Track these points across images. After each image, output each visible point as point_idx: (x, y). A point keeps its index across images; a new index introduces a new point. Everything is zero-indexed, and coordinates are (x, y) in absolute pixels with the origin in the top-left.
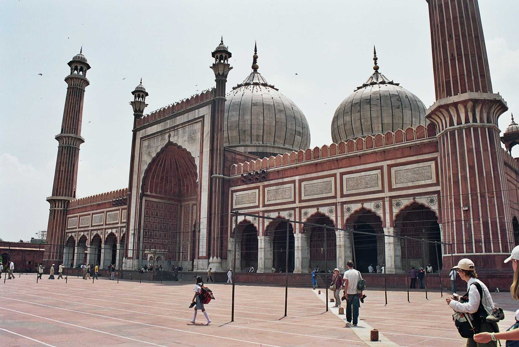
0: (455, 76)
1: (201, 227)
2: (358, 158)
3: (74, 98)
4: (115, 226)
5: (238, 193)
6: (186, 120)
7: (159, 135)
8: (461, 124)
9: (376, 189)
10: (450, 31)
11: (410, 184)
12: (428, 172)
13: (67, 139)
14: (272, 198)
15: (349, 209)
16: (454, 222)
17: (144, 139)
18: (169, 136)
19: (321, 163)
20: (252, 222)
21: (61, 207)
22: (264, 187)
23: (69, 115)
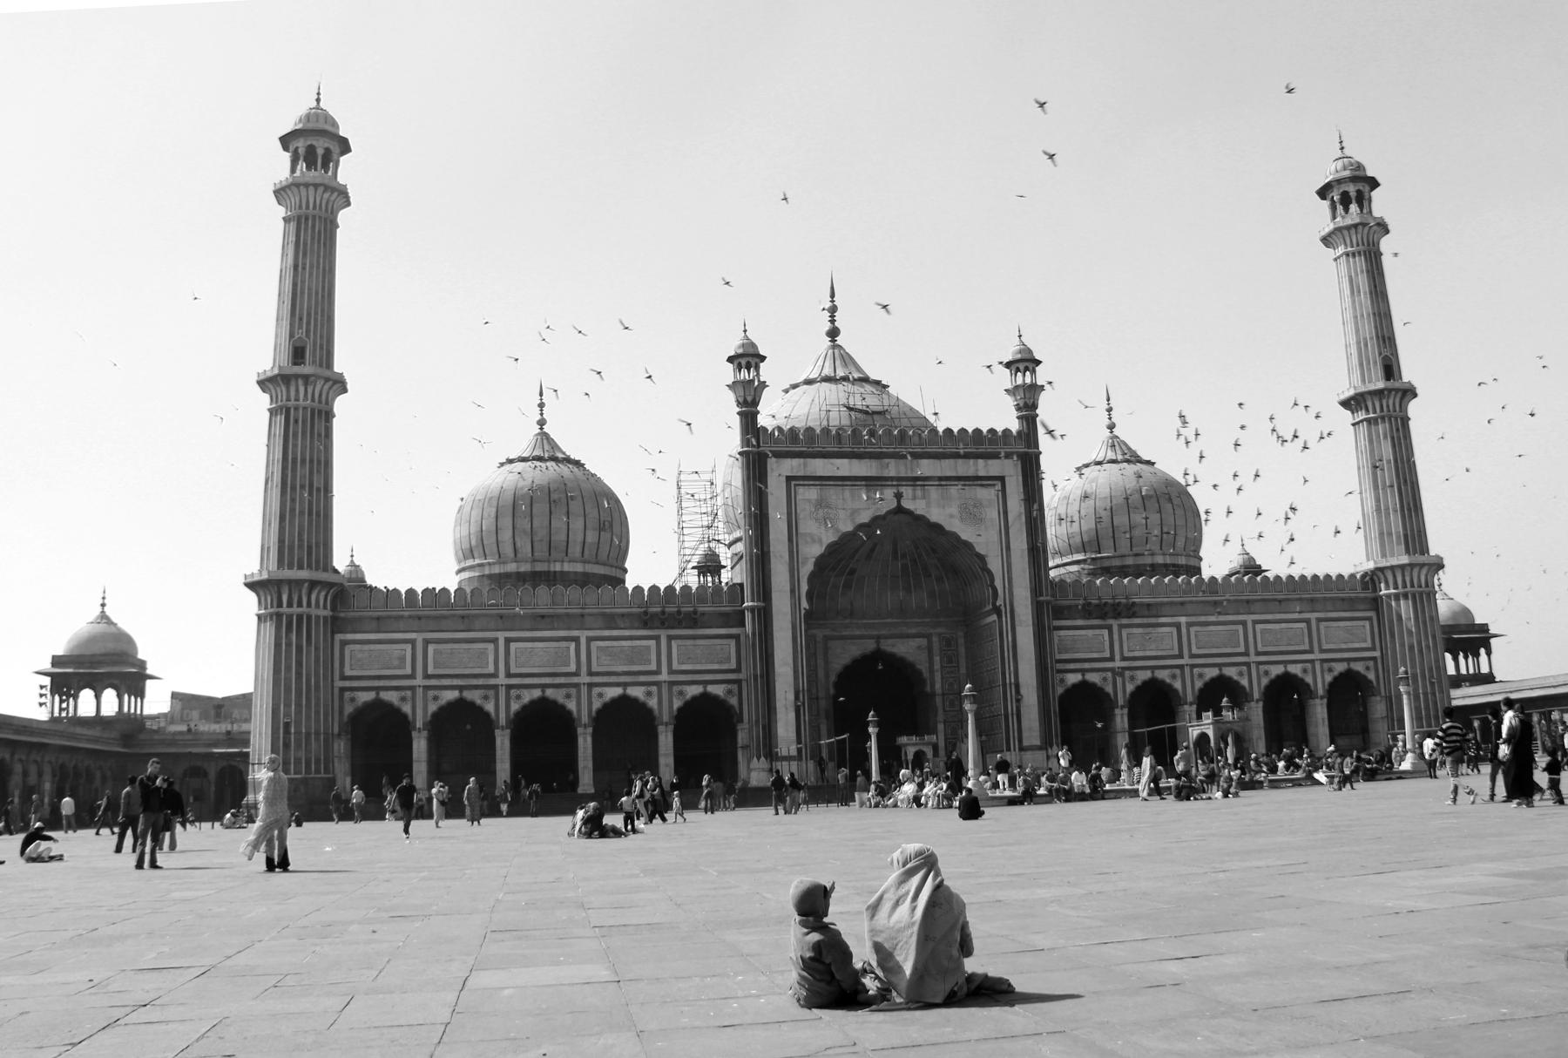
0: (1412, 530)
1: (1023, 691)
2: (1277, 603)
4: (642, 679)
5: (1062, 633)
6: (954, 474)
9: (1302, 648)
10: (1404, 474)
11: (1344, 646)
13: (326, 387)
15: (1266, 673)
16: (1421, 695)
17: (802, 483)
18: (899, 496)
21: (325, 607)
22: (1121, 626)
23: (323, 311)
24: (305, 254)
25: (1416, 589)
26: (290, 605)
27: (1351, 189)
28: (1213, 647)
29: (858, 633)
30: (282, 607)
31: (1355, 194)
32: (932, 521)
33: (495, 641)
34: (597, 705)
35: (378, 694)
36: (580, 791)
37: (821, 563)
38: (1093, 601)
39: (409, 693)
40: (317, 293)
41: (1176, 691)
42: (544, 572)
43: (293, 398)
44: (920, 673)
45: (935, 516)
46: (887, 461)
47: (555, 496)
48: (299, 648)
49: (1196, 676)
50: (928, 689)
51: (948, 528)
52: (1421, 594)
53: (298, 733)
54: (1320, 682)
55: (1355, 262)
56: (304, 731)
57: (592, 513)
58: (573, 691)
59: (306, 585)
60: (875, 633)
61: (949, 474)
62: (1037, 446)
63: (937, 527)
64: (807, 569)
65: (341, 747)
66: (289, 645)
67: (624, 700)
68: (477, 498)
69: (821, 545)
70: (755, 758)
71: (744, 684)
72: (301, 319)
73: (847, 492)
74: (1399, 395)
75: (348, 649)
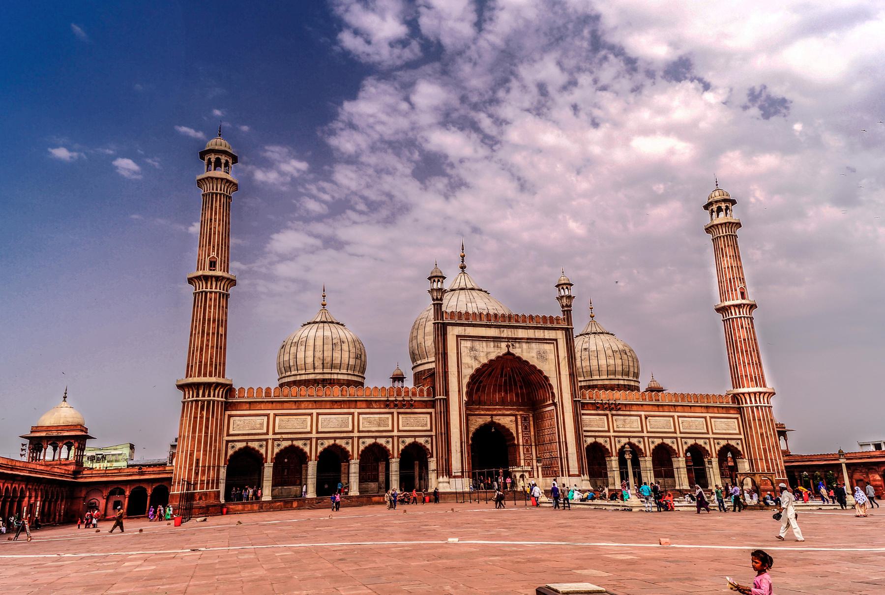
0: (759, 375)
3: (229, 214)
7: (490, 341)
8: (765, 403)
10: (753, 345)
11: (724, 432)
12: (733, 425)
14: (621, 426)
15: (686, 443)
16: (769, 460)
18: (508, 346)
19: (662, 405)
20: (603, 444)
21: (222, 397)
22: (613, 415)
23: (225, 243)
24: (216, 214)
25: (763, 404)
26: (203, 396)
27: (723, 206)
28: (658, 428)
29: (482, 413)
30: (199, 397)
31: (725, 207)
33: (311, 414)
34: (362, 447)
35: (247, 443)
36: (351, 494)
37: (473, 377)
38: (599, 402)
39: (265, 443)
40: (222, 235)
41: (641, 450)
42: (329, 379)
43: (209, 287)
44: (512, 434)
45: (525, 356)
47: (335, 341)
48: (207, 419)
49: (650, 443)
50: (516, 442)
52: (765, 407)
53: (204, 466)
54: (714, 449)
55: (724, 241)
56: (207, 465)
57: (353, 350)
58: (350, 441)
59: (214, 385)
60: (491, 413)
62: (572, 325)
63: (526, 362)
64: (466, 381)
65: (223, 472)
66: (201, 417)
67: (375, 445)
68: (294, 341)
71: (434, 437)
72: (214, 247)
73: (484, 344)
74: (749, 307)
75: (232, 419)
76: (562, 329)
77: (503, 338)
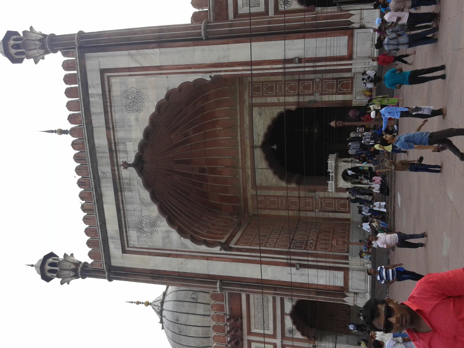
1: (290, 55)
6: (103, 116)
7: (122, 196)
18: (126, 165)
29: (249, 163)
32: (142, 138)
37: (182, 232)
44: (281, 115)
46: (100, 174)
50: (293, 108)
51: (148, 125)
60: (248, 149)
61: (103, 121)
63: (147, 133)
69: (171, 231)
70: (344, 299)
73: (128, 207)
76: (82, 59)
77: (114, 175)
